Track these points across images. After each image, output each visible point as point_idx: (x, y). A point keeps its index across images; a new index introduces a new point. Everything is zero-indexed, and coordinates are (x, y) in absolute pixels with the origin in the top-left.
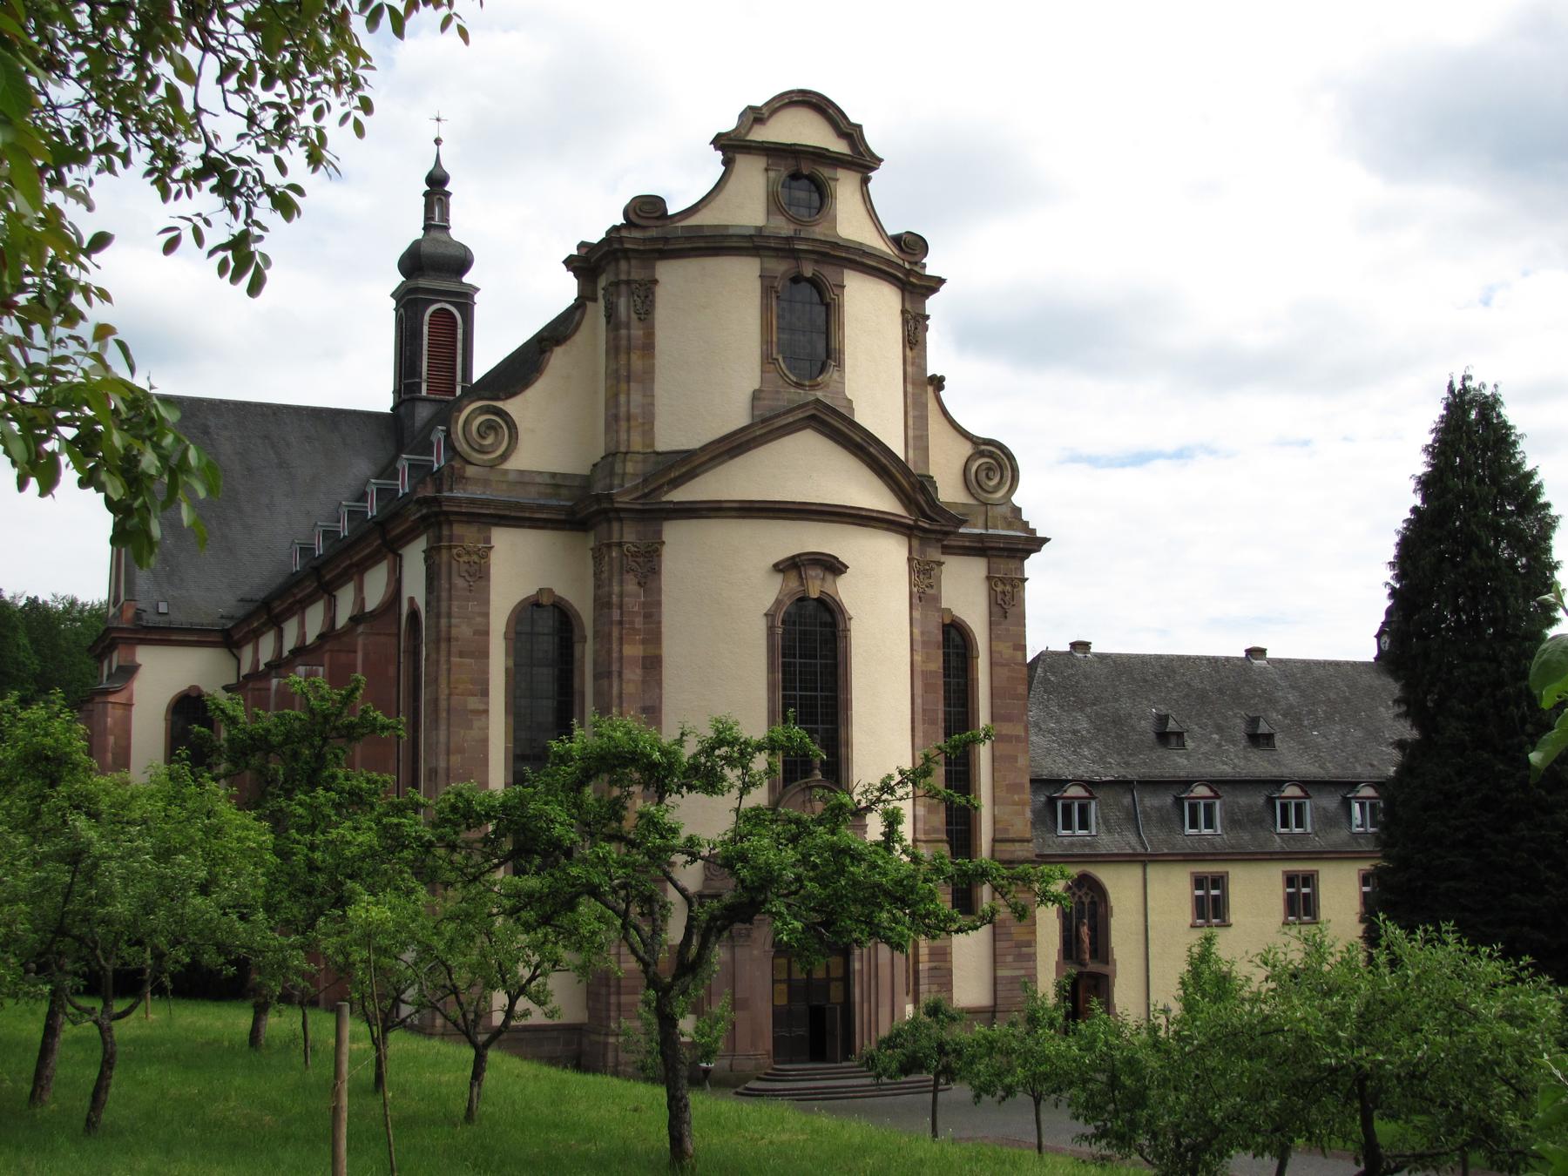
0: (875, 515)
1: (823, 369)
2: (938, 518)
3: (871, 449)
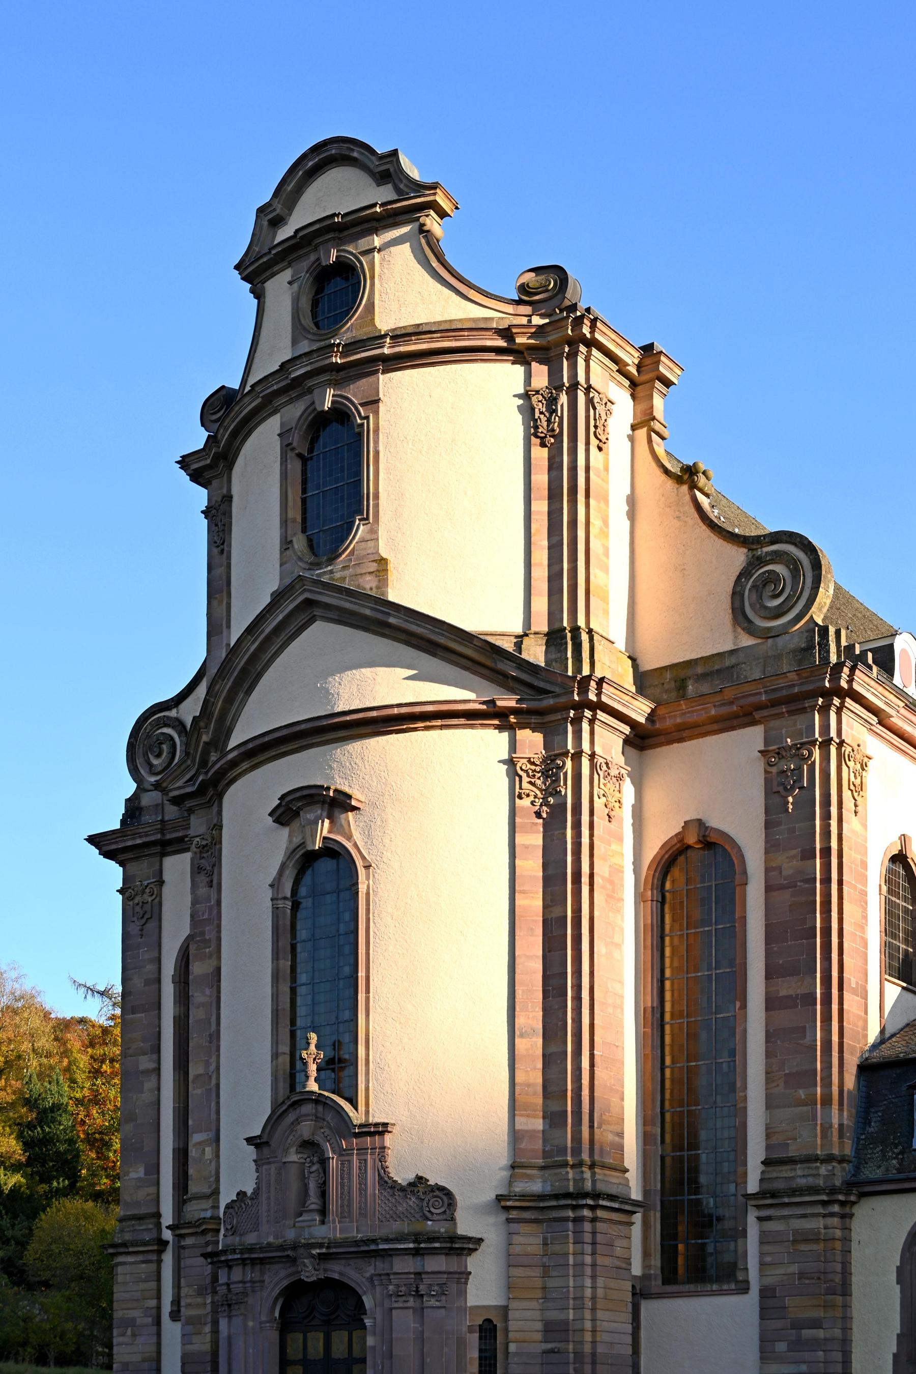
0: (396, 711)
1: (348, 527)
2: (548, 687)
3: (392, 620)
